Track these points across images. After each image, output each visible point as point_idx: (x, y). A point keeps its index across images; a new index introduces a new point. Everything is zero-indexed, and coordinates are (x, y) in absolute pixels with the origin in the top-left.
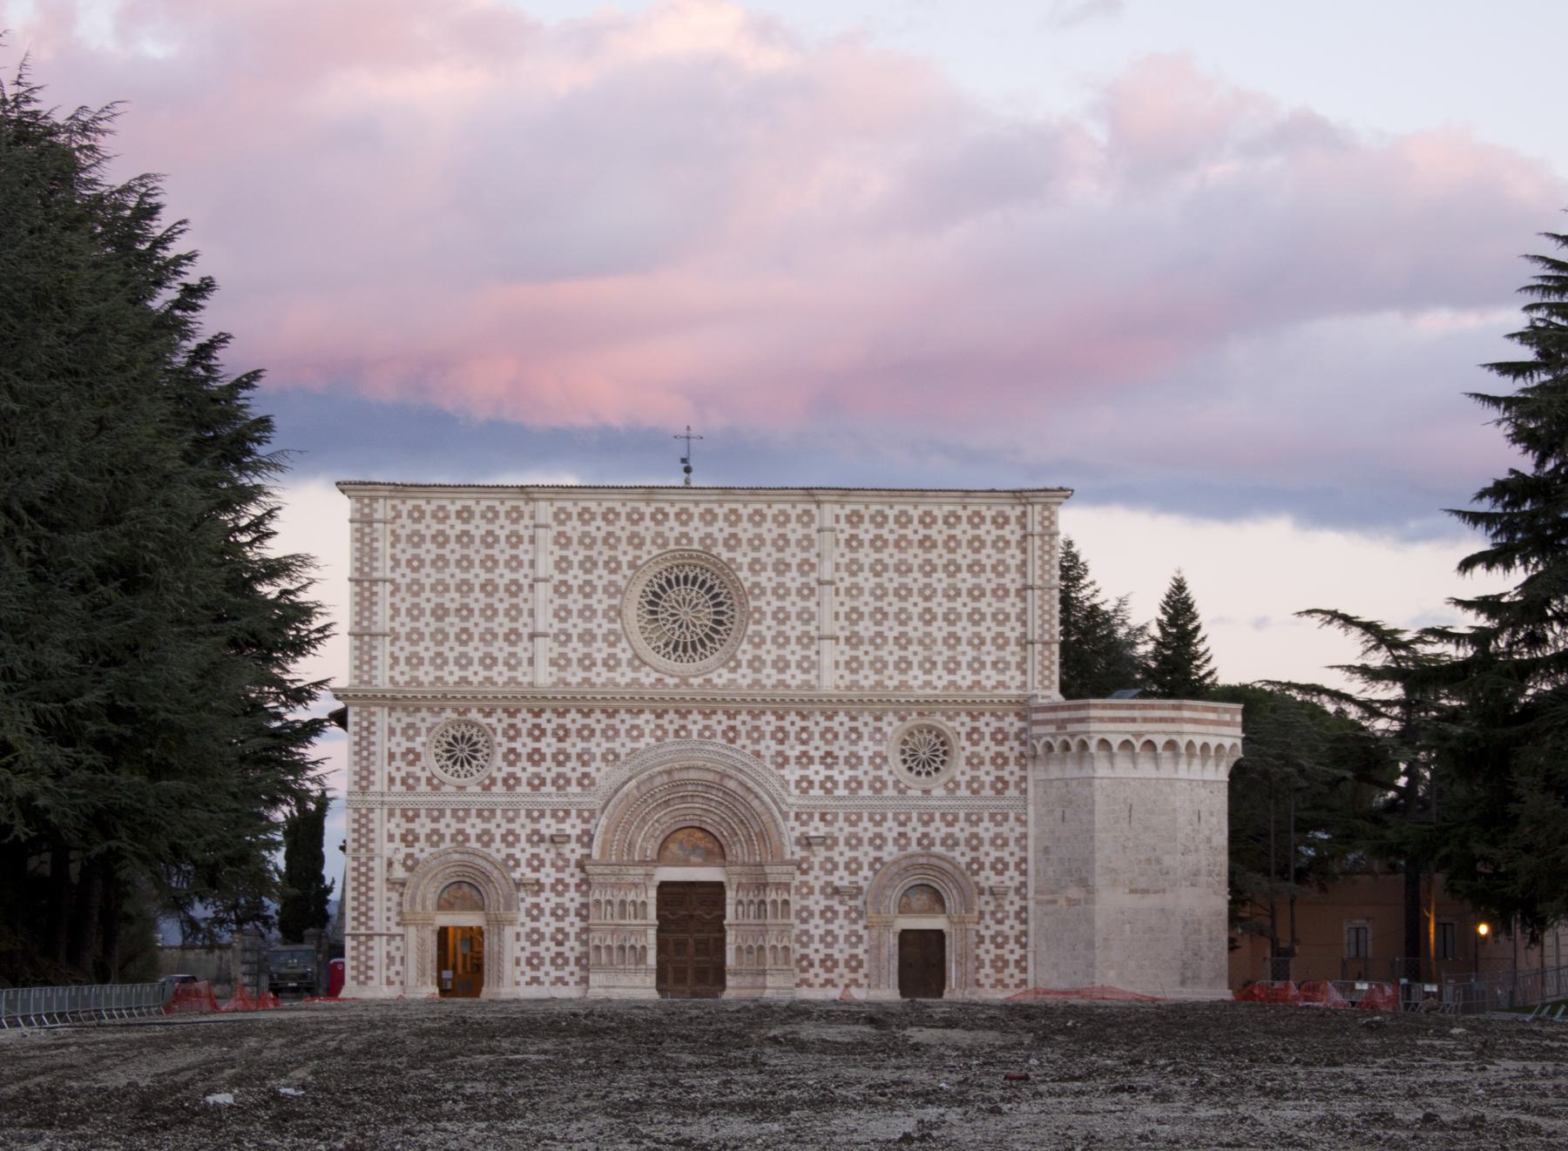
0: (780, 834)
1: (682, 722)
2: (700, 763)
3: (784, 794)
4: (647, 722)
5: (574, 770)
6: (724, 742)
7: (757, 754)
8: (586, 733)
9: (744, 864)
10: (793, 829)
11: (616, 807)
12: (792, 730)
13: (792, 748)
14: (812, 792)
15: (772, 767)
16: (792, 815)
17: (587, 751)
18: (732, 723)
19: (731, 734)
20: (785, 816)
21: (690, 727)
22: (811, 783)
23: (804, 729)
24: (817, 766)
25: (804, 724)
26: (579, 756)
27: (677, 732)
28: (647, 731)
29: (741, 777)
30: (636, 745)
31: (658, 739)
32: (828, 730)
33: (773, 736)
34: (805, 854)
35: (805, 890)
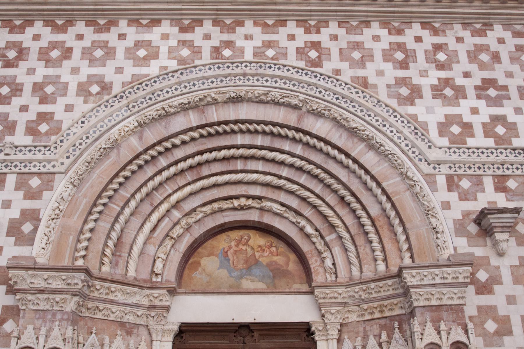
0: (428, 212)
1: (226, 37)
2: (260, 90)
3: (422, 145)
4: (165, 37)
5: (24, 109)
6: (302, 64)
7: (364, 83)
8: (55, 54)
9: (351, 283)
10: (446, 205)
11: (91, 165)
12: (420, 49)
13: (424, 74)
14: (471, 142)
15: (393, 103)
16: (441, 181)
17: (55, 80)
18: (314, 37)
19: (313, 54)
20: (430, 179)
21: (239, 43)
22: (467, 127)
23: (438, 48)
24: (472, 101)
25: (439, 40)
26: (37, 88)
27: (216, 51)
28: (164, 50)
29: (336, 112)
30: (144, 70)
31: (181, 61)
32: (480, 48)
33: (387, 56)
34: (479, 252)
35: (491, 326)
